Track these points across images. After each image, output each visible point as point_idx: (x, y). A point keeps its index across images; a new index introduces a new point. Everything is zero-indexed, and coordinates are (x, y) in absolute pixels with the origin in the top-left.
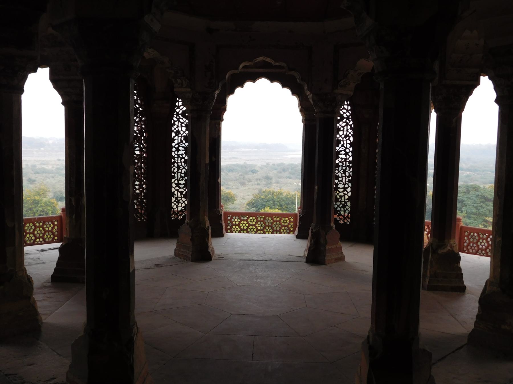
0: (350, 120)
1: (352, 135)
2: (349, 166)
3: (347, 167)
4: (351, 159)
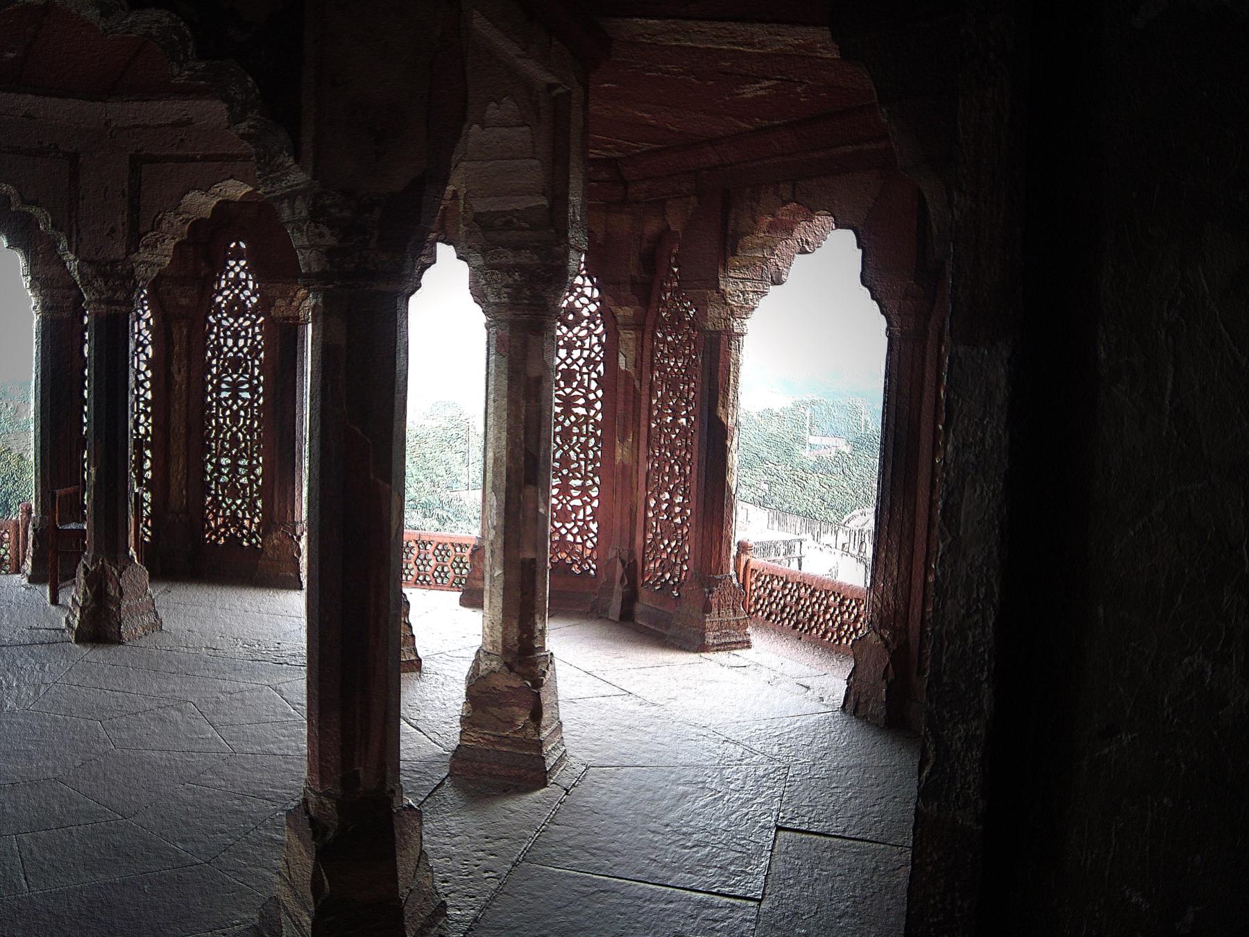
0: (146, 308)
1: (150, 343)
2: (145, 412)
3: (142, 413)
4: (149, 395)
